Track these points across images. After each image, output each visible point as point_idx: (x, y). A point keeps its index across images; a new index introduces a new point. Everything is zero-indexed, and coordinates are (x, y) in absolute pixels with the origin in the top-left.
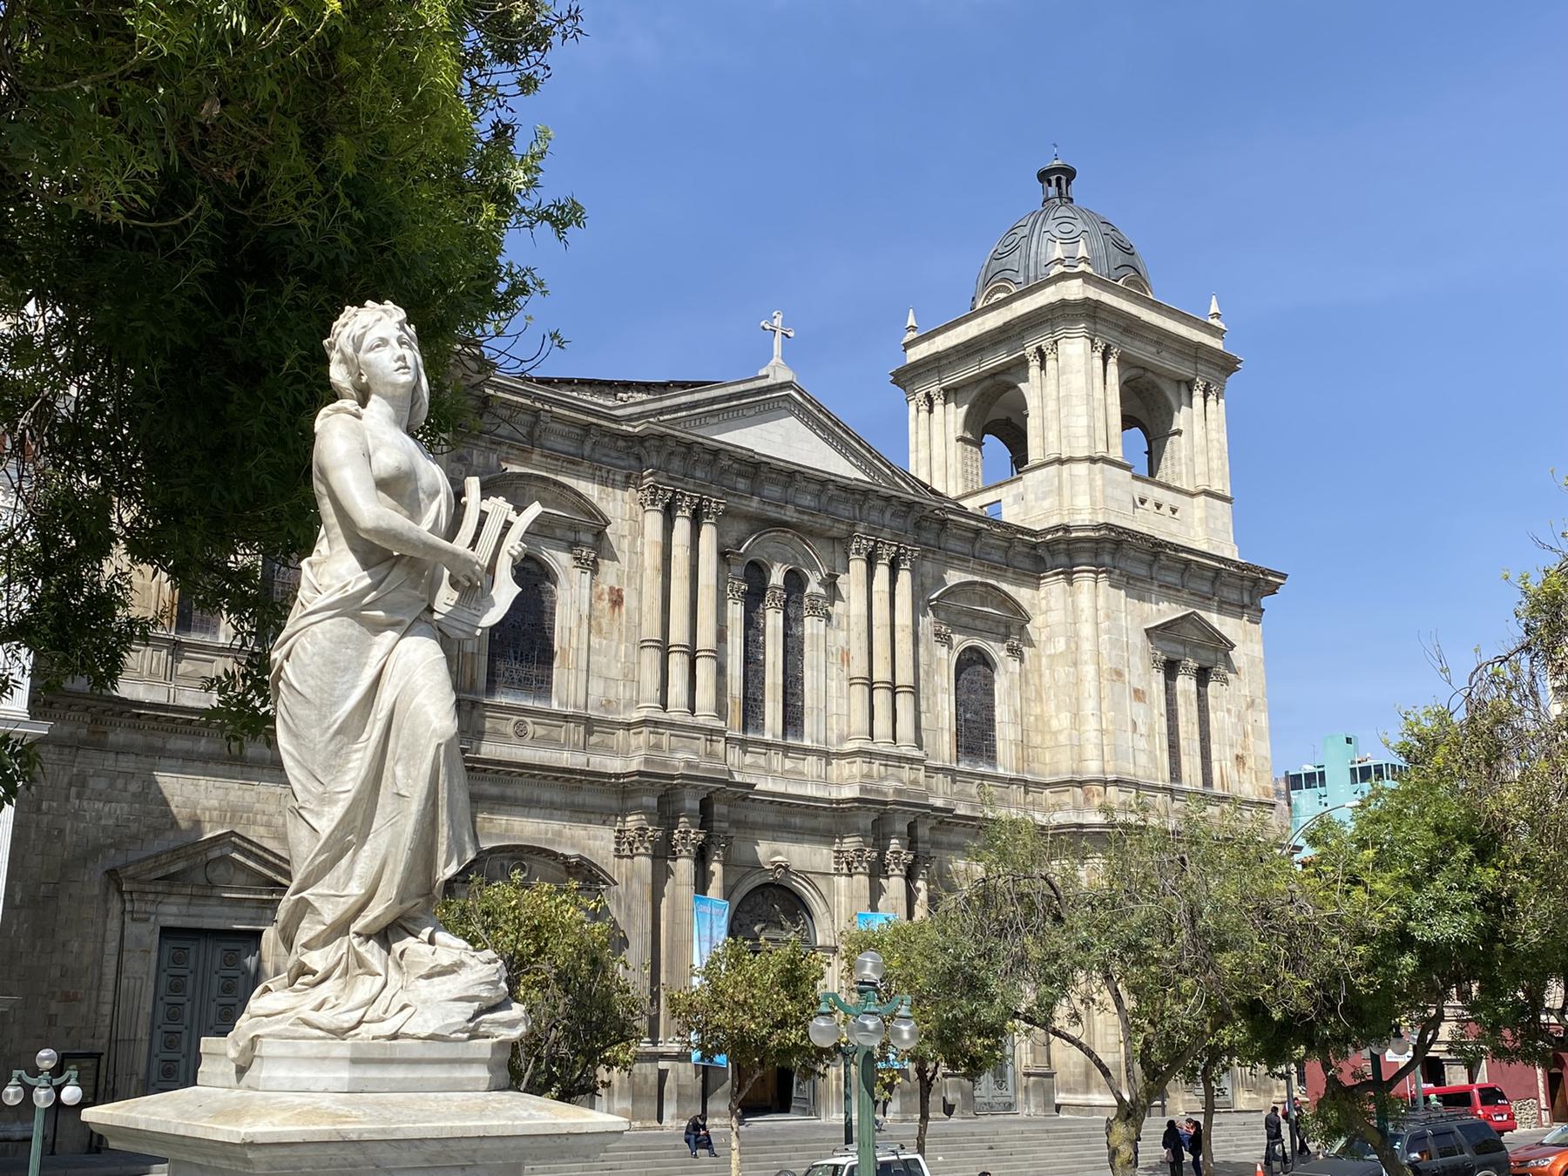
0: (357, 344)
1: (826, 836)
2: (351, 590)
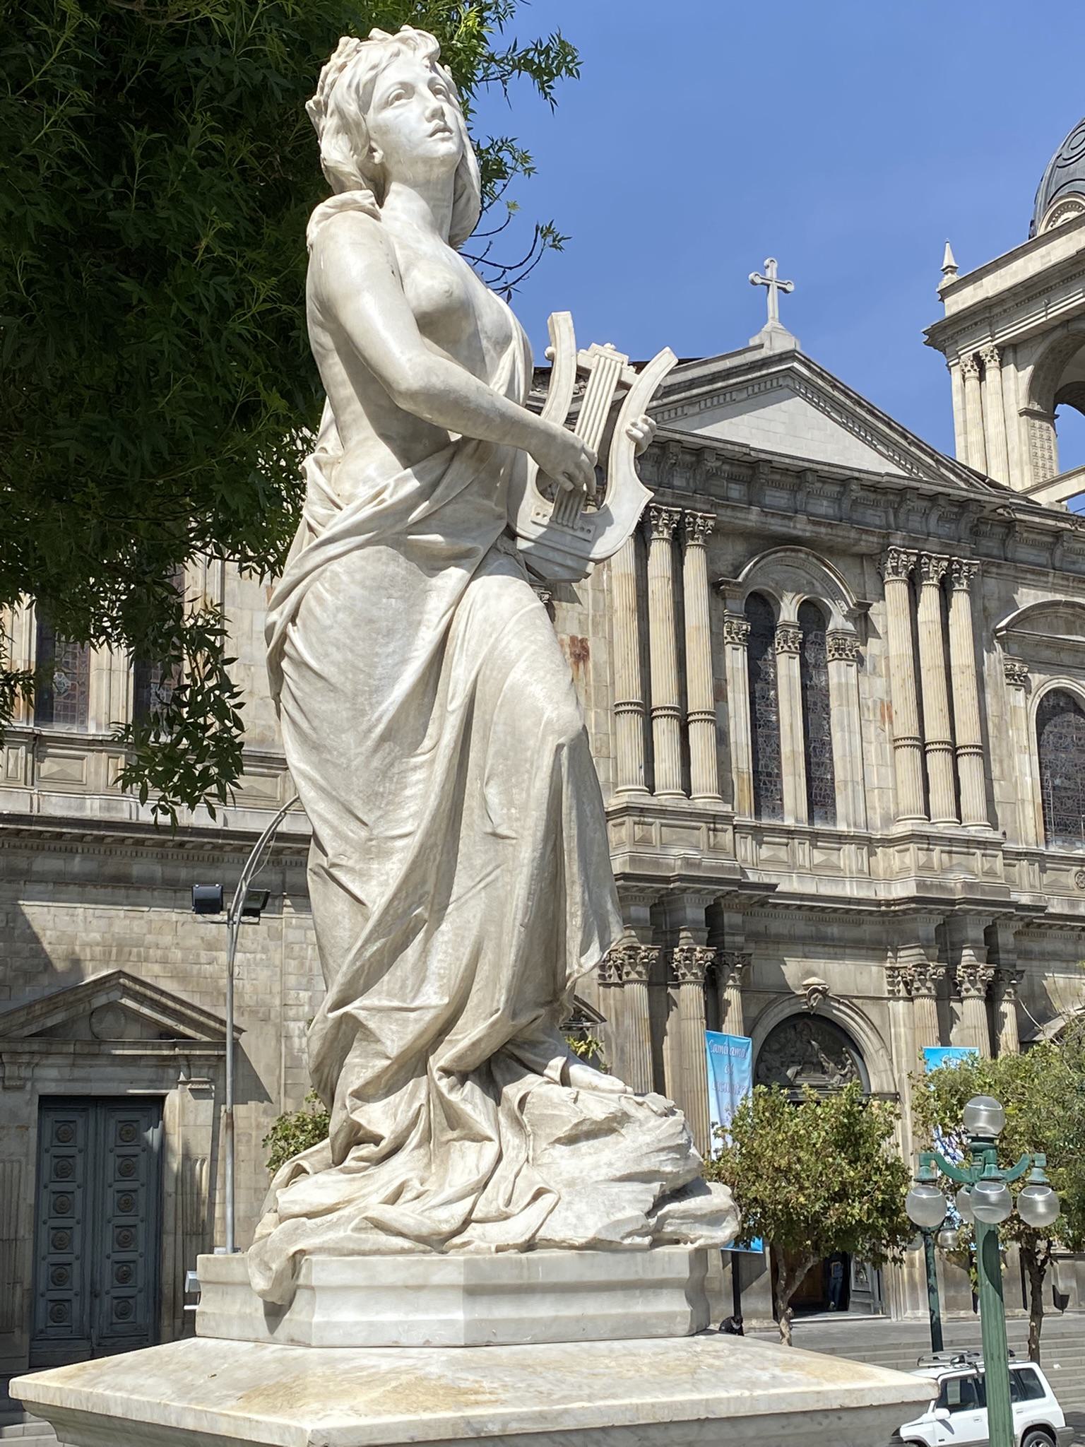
0: (364, 97)
1: (875, 948)
2: (389, 499)
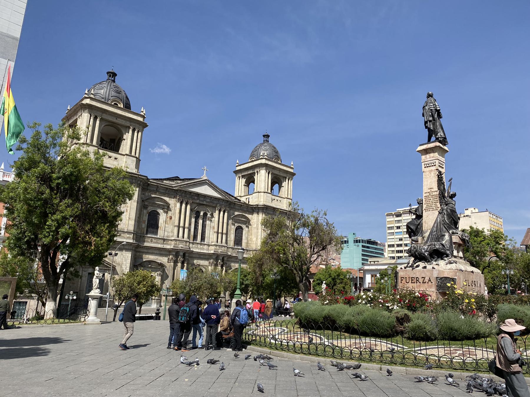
1: (207, 259)
